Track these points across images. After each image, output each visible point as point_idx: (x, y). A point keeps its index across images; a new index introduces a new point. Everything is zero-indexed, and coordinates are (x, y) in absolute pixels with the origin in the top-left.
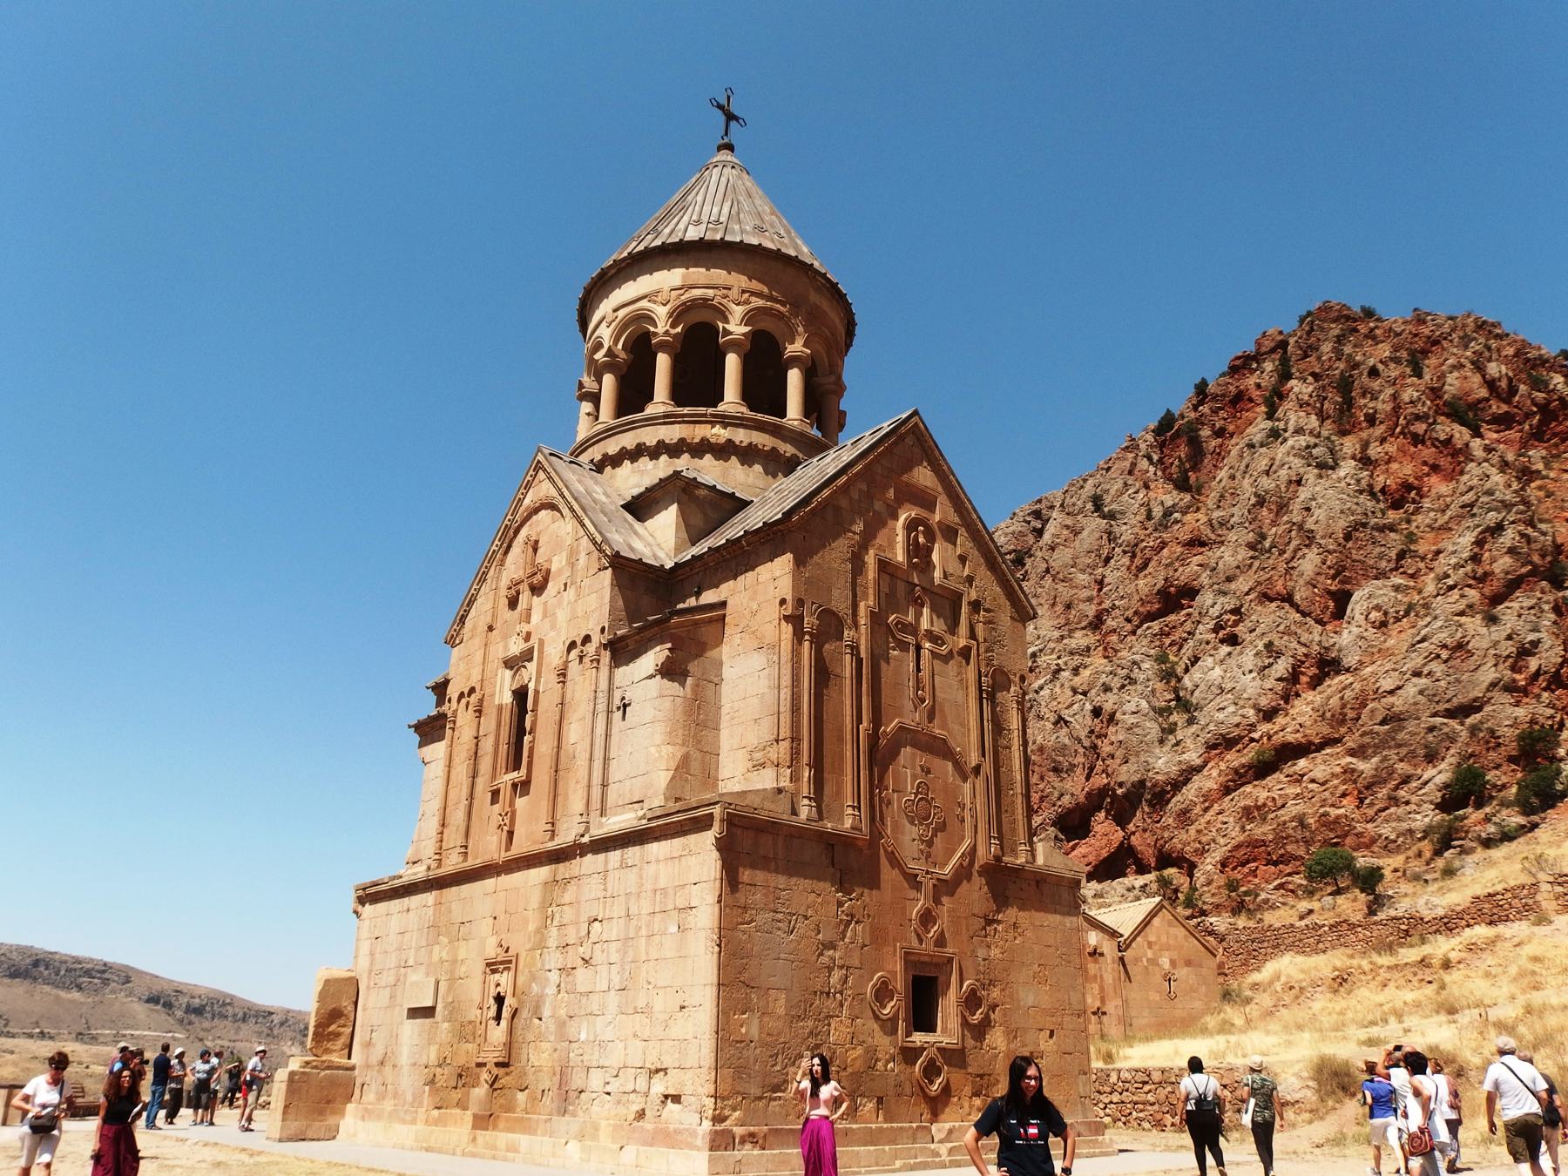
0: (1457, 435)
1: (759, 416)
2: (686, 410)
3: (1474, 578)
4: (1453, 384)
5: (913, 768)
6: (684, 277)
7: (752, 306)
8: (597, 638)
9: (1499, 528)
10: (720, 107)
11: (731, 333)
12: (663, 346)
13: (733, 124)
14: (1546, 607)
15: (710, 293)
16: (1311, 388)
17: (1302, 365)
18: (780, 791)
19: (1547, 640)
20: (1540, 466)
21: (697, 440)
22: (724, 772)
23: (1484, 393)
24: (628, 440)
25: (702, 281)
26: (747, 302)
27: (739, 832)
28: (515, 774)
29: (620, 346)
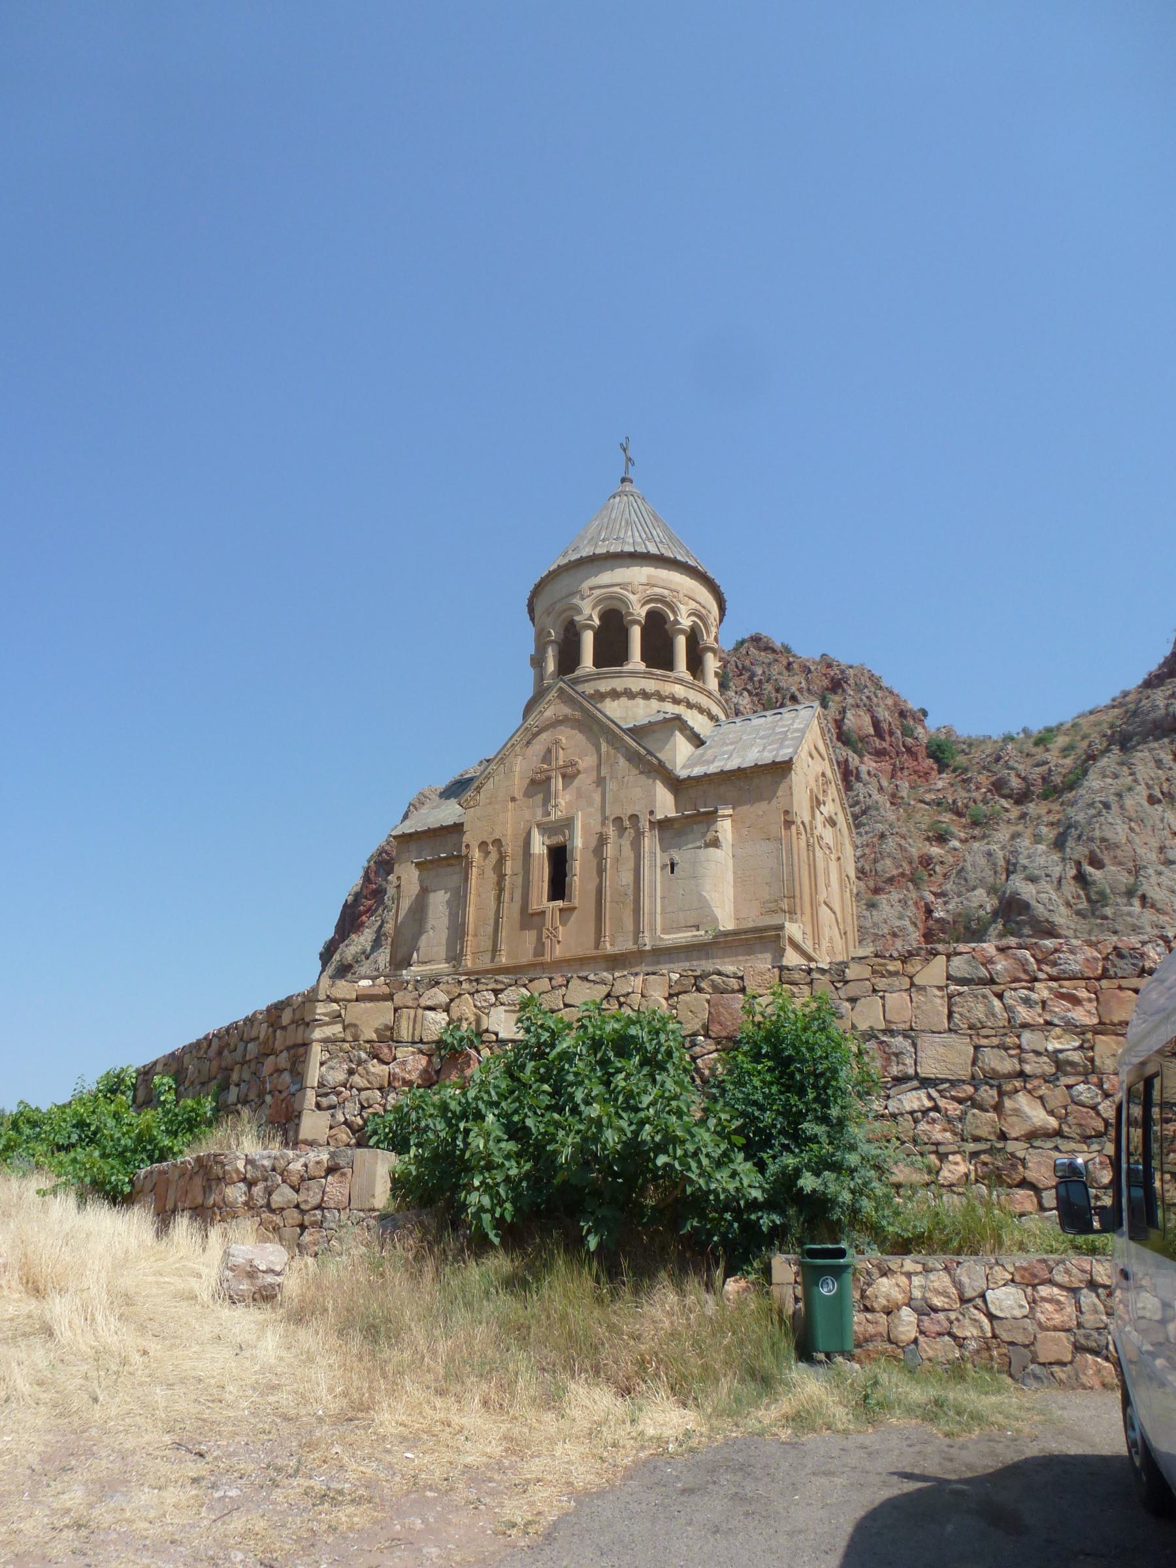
0: (850, 759)
2: (659, 672)
3: (863, 873)
4: (850, 720)
6: (649, 577)
9: (882, 836)
11: (680, 624)
14: (910, 903)
16: (745, 702)
17: (737, 681)
19: (911, 929)
20: (904, 794)
23: (871, 731)
24: (618, 684)
26: (687, 604)
28: (560, 903)
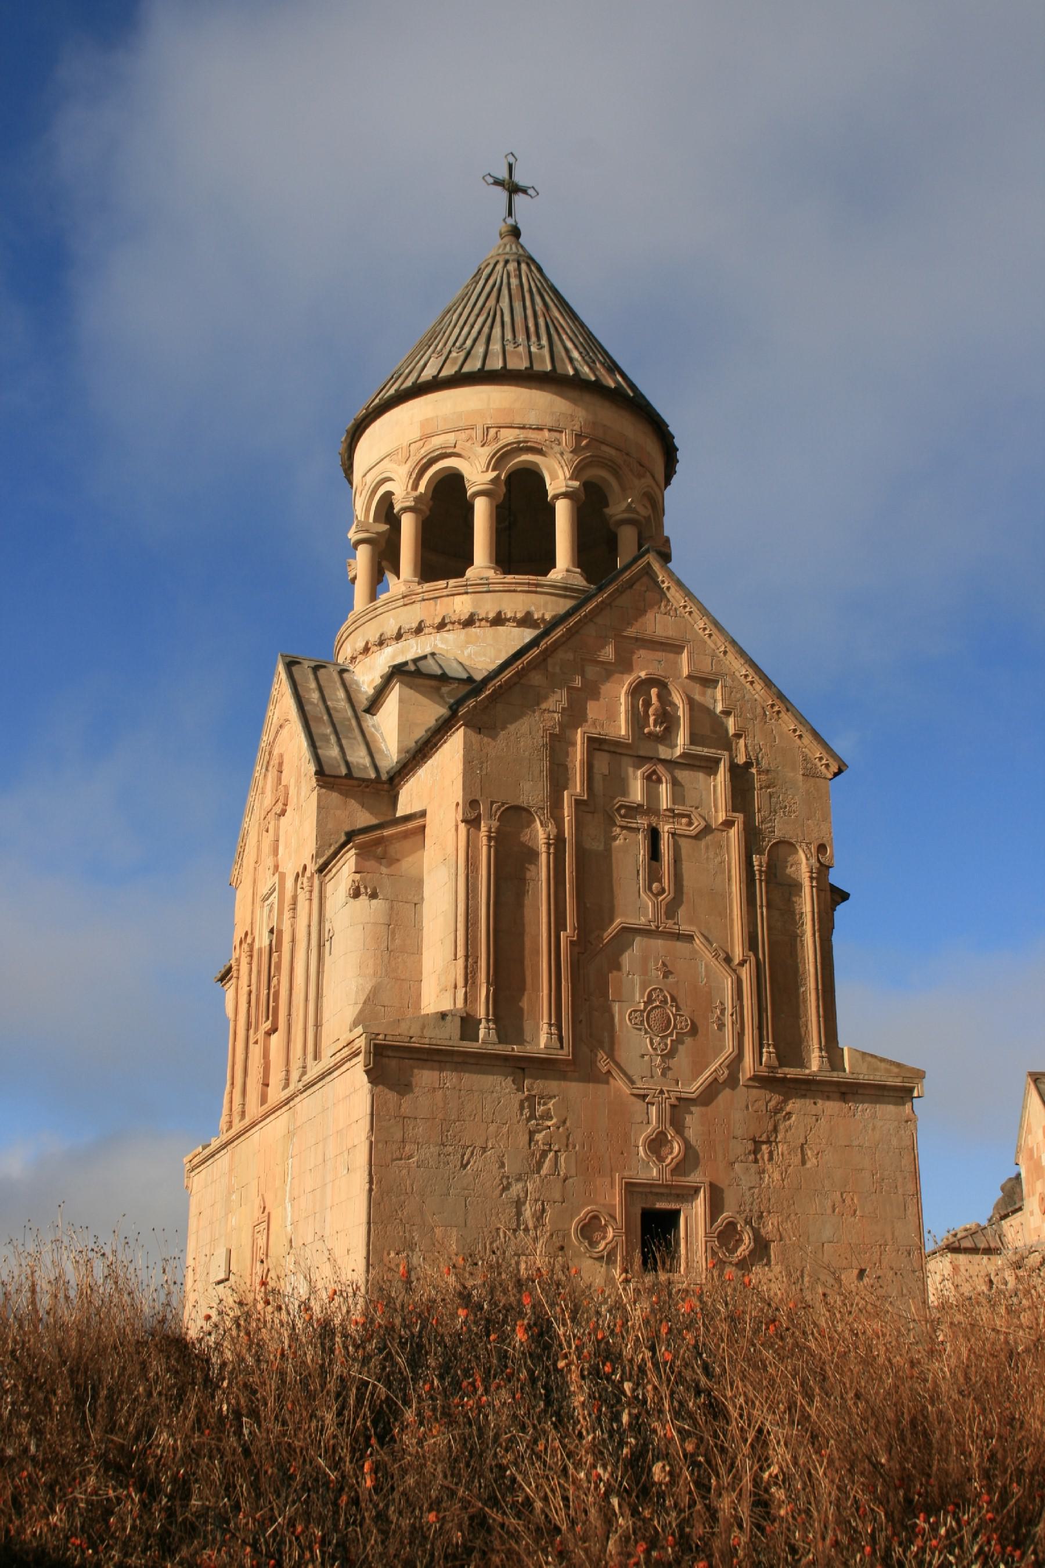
1: (509, 578)
2: (427, 586)
5: (645, 972)
6: (423, 424)
7: (501, 443)
8: (312, 868)
10: (498, 182)
12: (405, 510)
13: (519, 199)
15: (451, 438)
18: (443, 1015)
21: (438, 620)
22: (424, 1002)
25: (442, 426)
27: (394, 1063)
29: (371, 520)
